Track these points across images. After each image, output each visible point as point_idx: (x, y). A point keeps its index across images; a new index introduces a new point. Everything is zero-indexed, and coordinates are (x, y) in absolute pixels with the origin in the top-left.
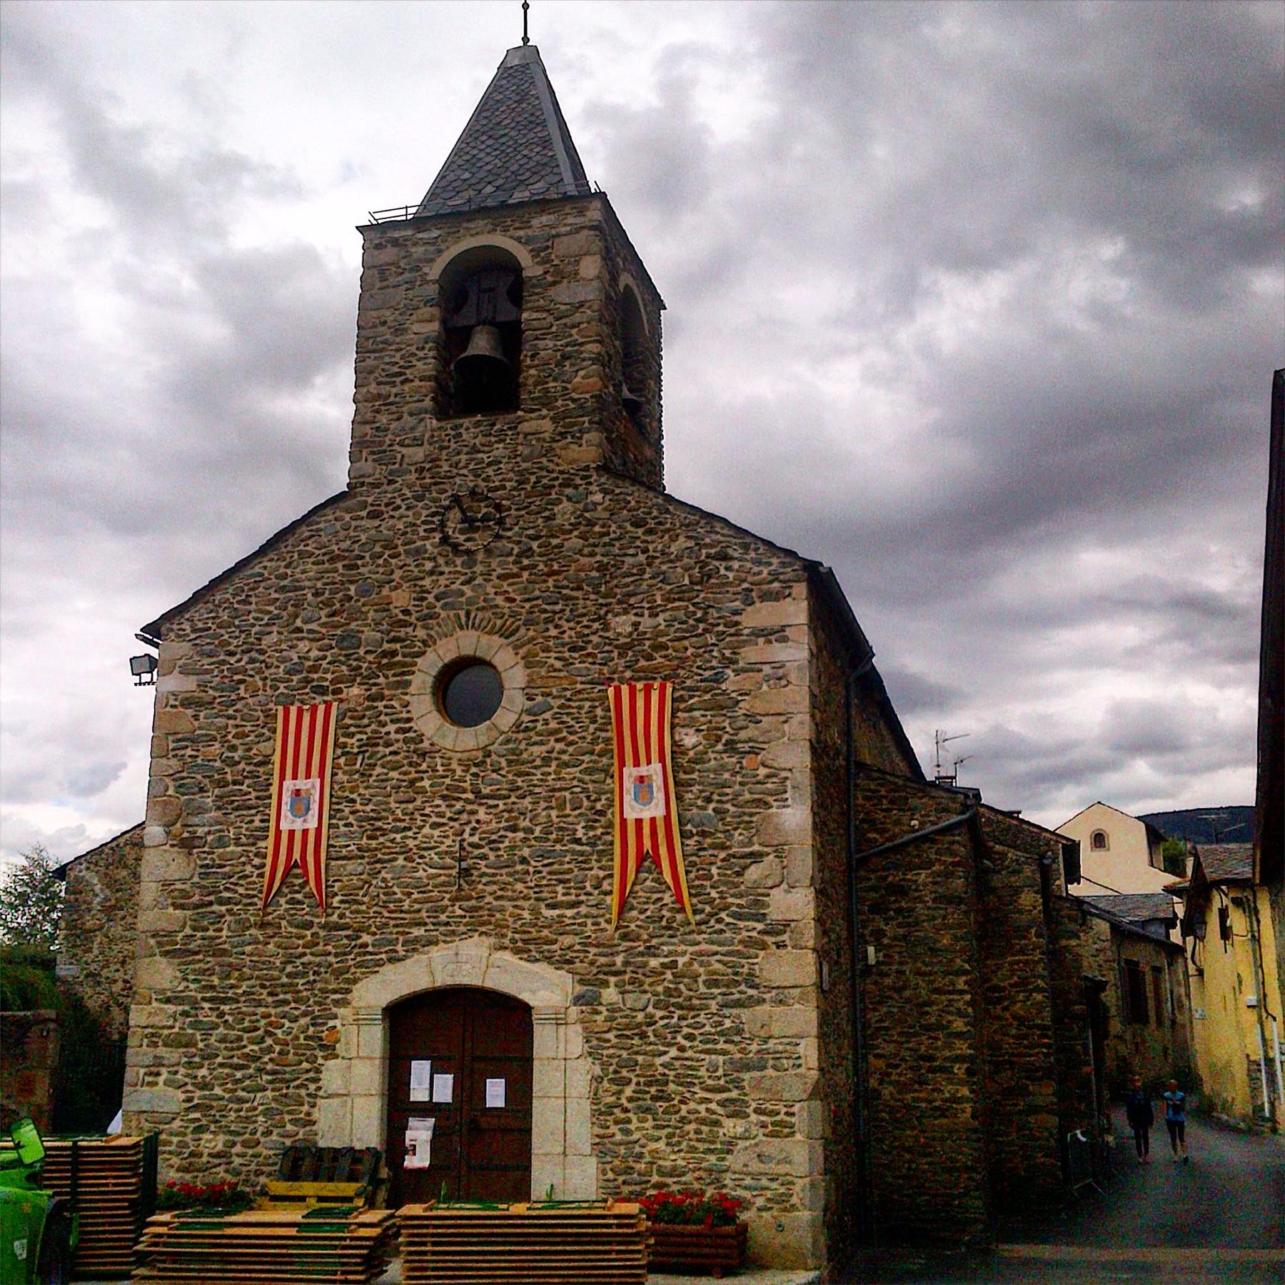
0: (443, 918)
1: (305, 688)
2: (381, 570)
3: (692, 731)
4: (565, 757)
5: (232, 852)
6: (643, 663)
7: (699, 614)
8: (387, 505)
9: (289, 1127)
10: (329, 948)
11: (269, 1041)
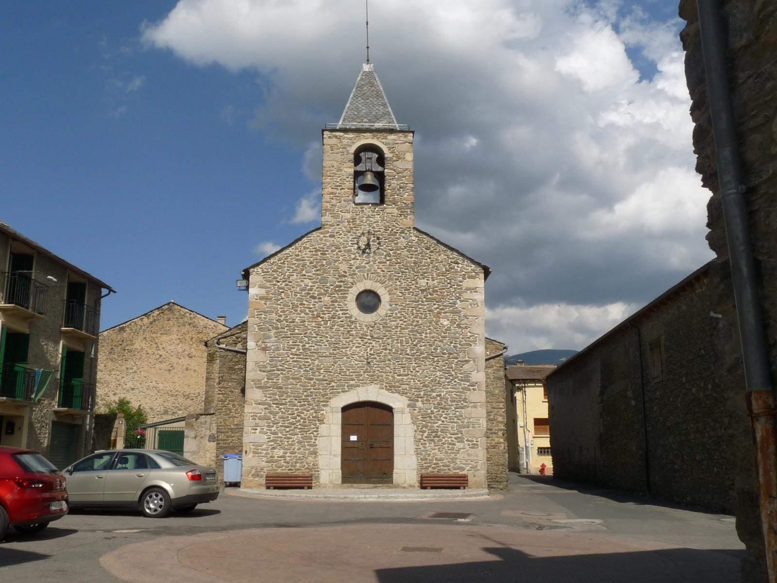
0: (361, 378)
1: (307, 296)
2: (335, 256)
3: (446, 320)
4: (403, 326)
5: (282, 353)
6: (429, 296)
7: (449, 281)
8: (337, 233)
9: (307, 447)
10: (320, 387)
11: (298, 418)
